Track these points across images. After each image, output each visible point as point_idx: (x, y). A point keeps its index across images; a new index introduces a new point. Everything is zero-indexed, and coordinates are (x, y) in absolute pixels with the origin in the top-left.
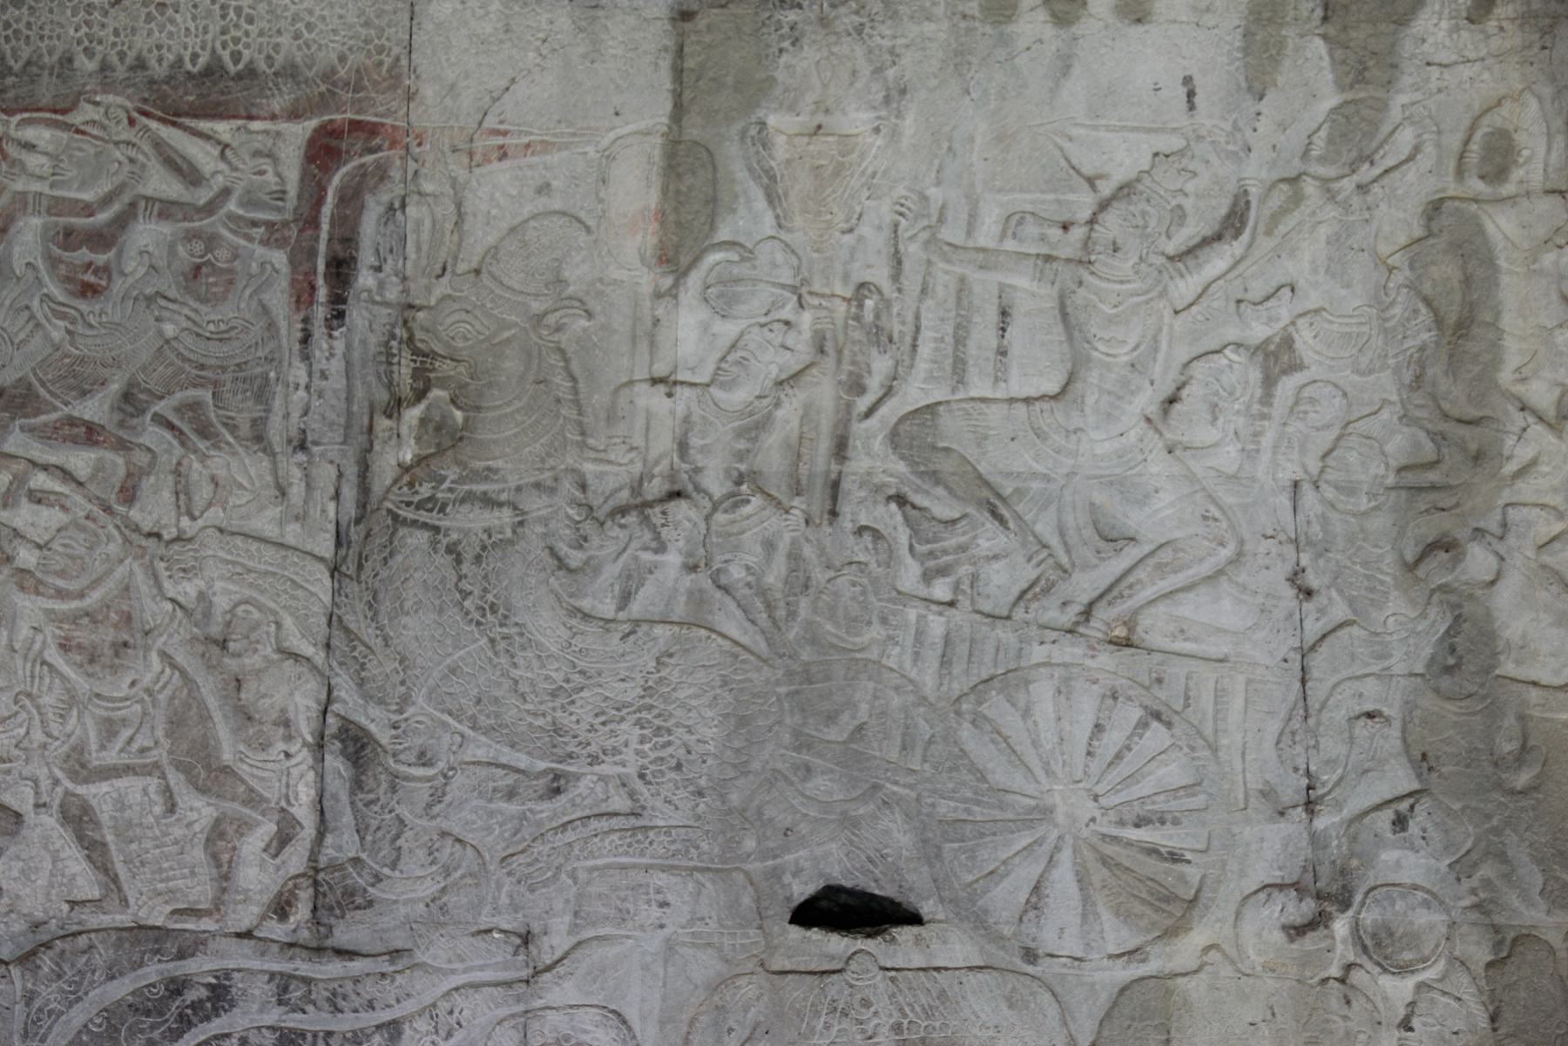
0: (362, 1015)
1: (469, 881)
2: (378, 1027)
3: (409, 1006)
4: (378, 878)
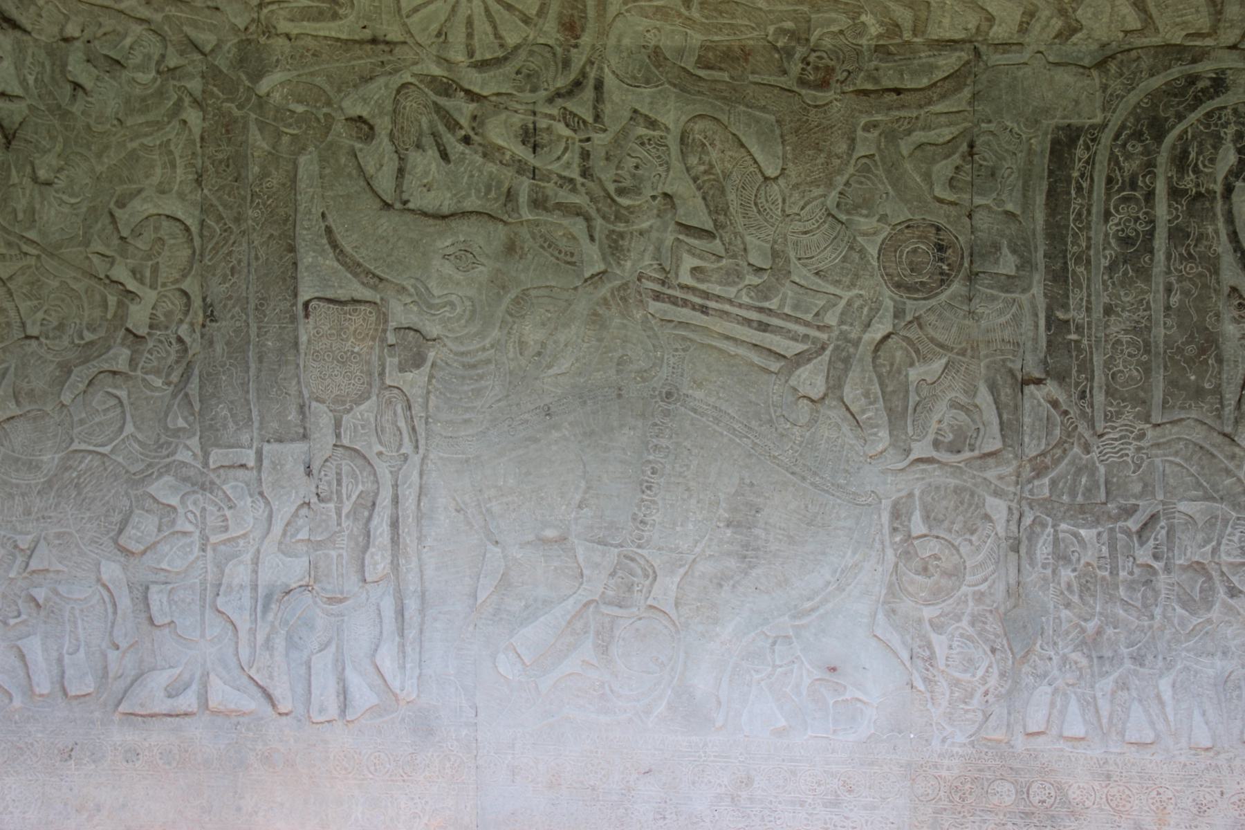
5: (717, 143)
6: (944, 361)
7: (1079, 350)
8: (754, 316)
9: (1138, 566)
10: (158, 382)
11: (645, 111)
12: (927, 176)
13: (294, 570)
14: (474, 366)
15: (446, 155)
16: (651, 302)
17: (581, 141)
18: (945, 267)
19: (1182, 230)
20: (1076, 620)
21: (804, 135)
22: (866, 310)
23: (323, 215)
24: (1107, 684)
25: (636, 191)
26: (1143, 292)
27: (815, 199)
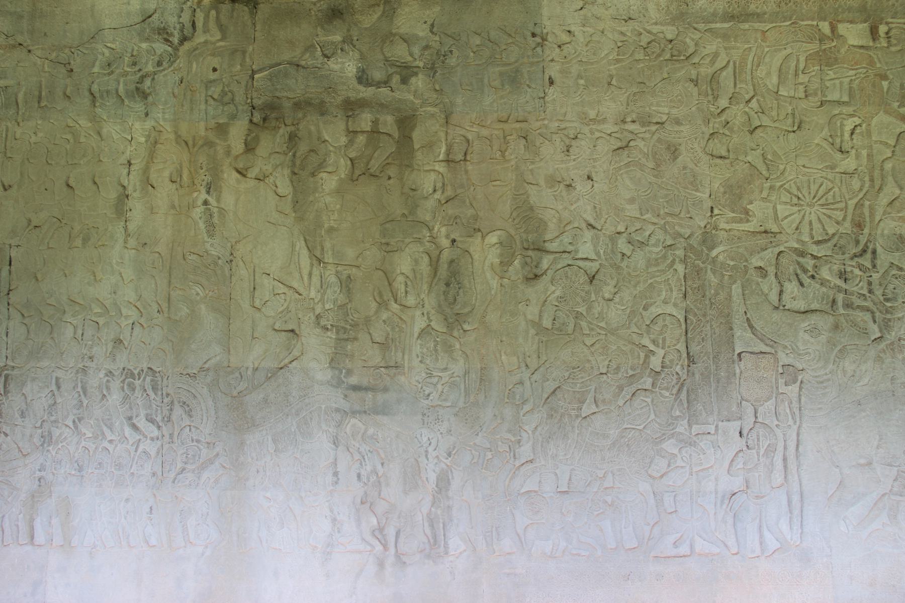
10: (667, 394)
13: (737, 483)
14: (822, 382)
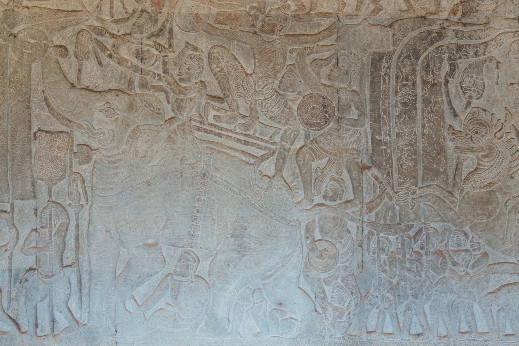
0: (478, 40)
1: (503, 5)
2: (482, 43)
3: (489, 38)
4: (479, 5)
5: (225, 58)
6: (327, 158)
7: (386, 152)
8: (242, 138)
9: (414, 252)
11: (192, 43)
12: (318, 74)
14: (114, 162)
15: (101, 63)
16: (196, 132)
17: (163, 57)
18: (327, 115)
19: (428, 100)
20: (388, 278)
21: (263, 55)
22: (292, 135)
23: (43, 91)
24: (402, 308)
25: (188, 80)
26: (412, 127)
27: (269, 84)
